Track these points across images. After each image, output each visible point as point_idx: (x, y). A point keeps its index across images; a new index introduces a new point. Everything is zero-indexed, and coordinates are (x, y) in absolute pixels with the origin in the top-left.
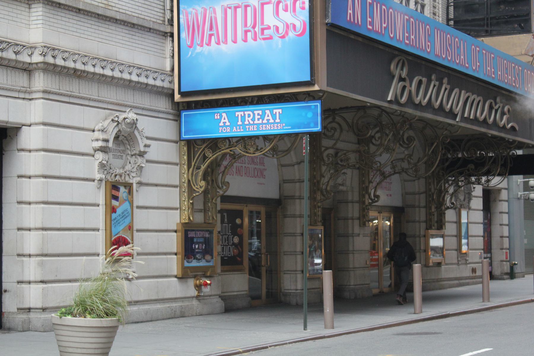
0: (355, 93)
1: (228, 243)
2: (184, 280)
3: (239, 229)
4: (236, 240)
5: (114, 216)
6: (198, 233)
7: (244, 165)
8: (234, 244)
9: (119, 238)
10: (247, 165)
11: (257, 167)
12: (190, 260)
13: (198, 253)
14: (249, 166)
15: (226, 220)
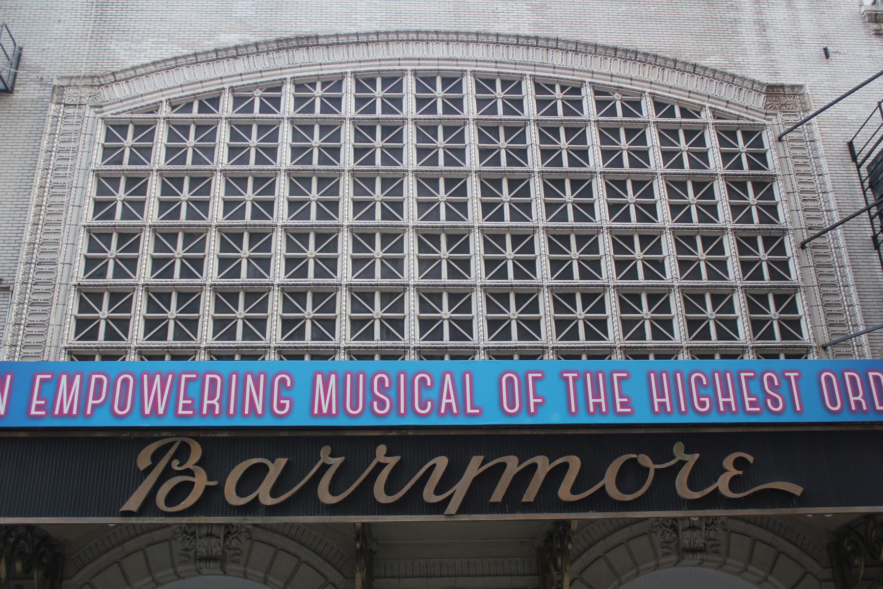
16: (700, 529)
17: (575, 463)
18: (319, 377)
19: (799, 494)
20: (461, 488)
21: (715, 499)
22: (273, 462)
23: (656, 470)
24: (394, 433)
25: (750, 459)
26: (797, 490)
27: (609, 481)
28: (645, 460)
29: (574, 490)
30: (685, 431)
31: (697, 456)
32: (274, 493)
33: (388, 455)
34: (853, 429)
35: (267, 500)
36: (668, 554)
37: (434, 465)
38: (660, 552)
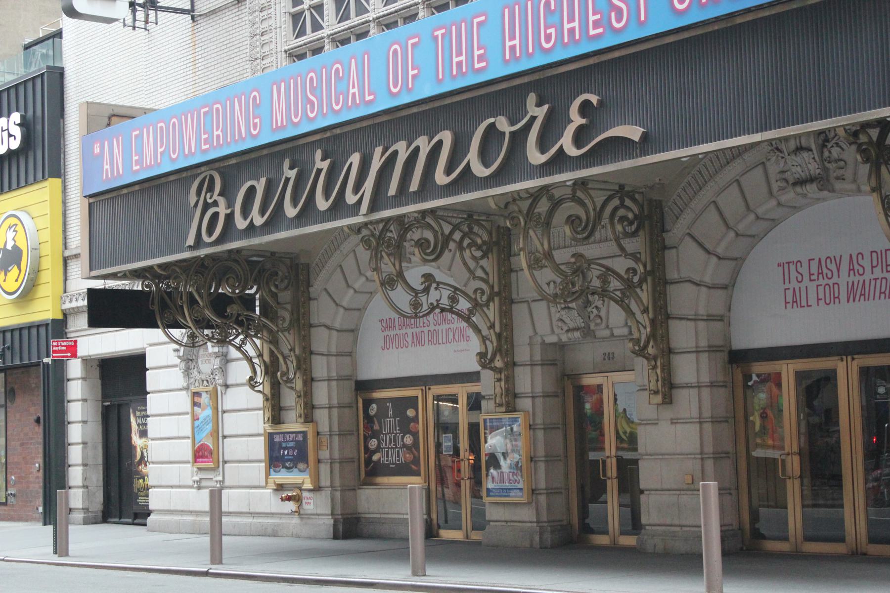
0: (133, 262)
1: (395, 445)
2: (318, 493)
3: (412, 424)
4: (408, 439)
5: (197, 423)
6: (288, 436)
7: (426, 329)
8: (404, 446)
9: (202, 445)
10: (432, 328)
11: (451, 326)
12: (278, 469)
13: (288, 460)
14: (437, 327)
15: (391, 413)
16: (809, 150)
17: (447, 137)
18: (275, 87)
19: (636, 138)
20: (369, 185)
21: (560, 161)
22: (258, 180)
23: (510, 133)
24: (328, 134)
25: (594, 99)
26: (634, 133)
27: (472, 157)
28: (503, 125)
29: (448, 171)
30: (536, 77)
31: (546, 107)
32: (262, 212)
33: (323, 160)
34: (710, 29)
35: (259, 221)
36: (783, 189)
37: (351, 164)
38: (775, 186)
